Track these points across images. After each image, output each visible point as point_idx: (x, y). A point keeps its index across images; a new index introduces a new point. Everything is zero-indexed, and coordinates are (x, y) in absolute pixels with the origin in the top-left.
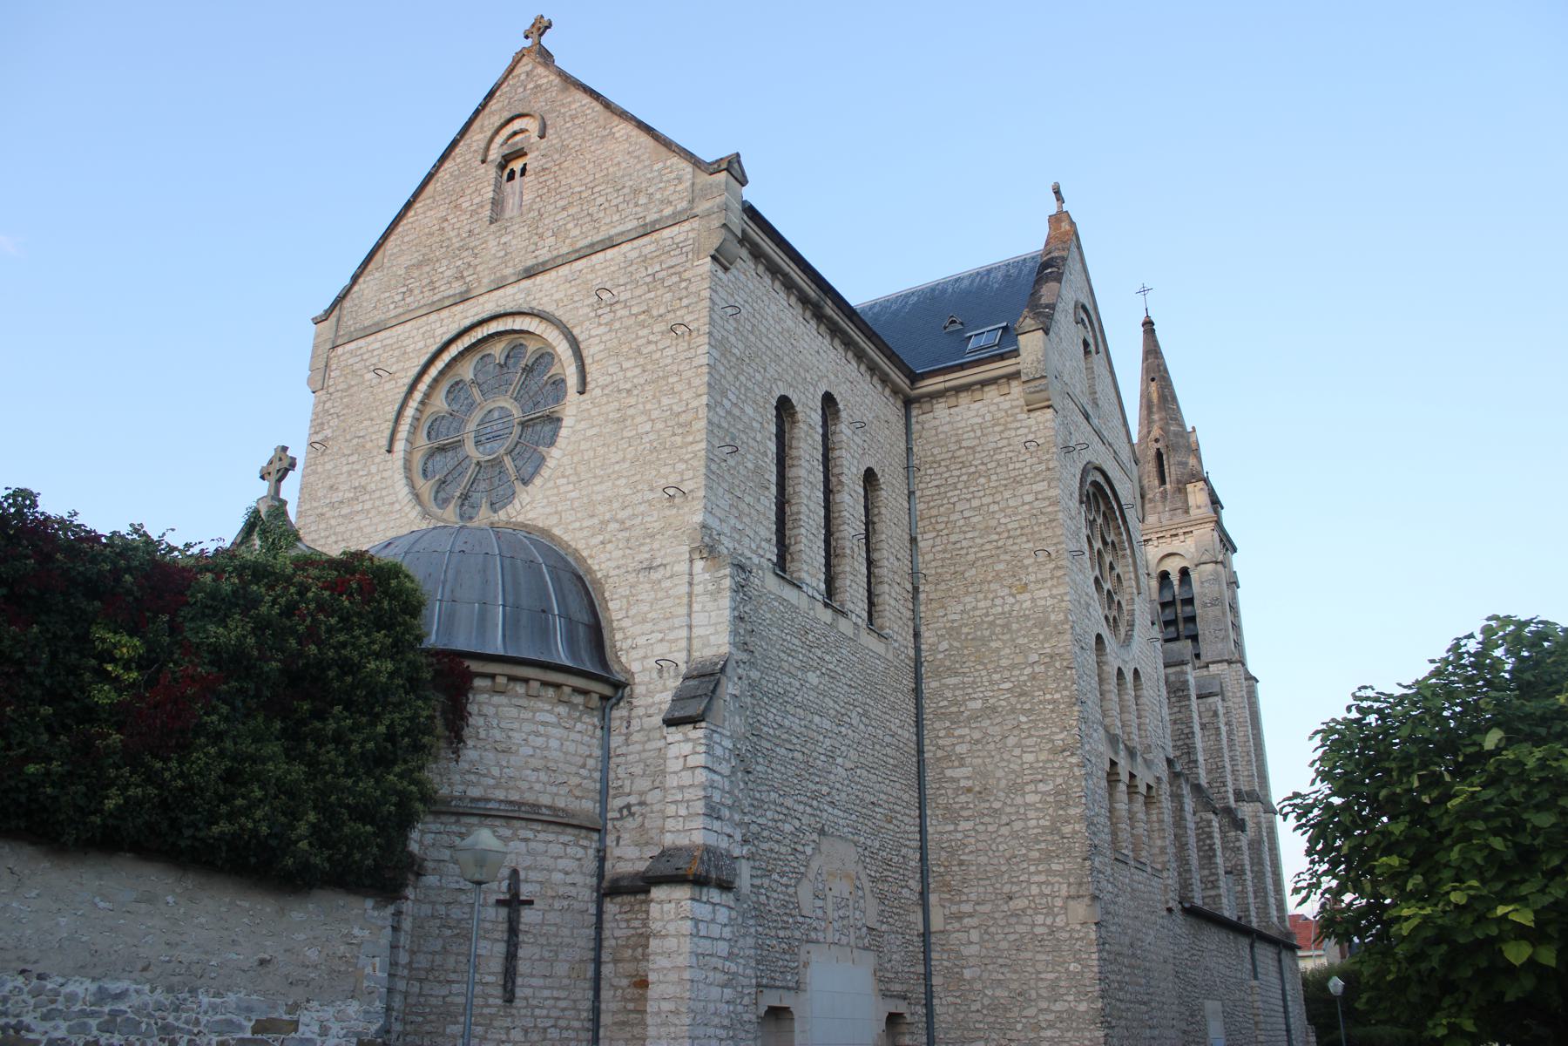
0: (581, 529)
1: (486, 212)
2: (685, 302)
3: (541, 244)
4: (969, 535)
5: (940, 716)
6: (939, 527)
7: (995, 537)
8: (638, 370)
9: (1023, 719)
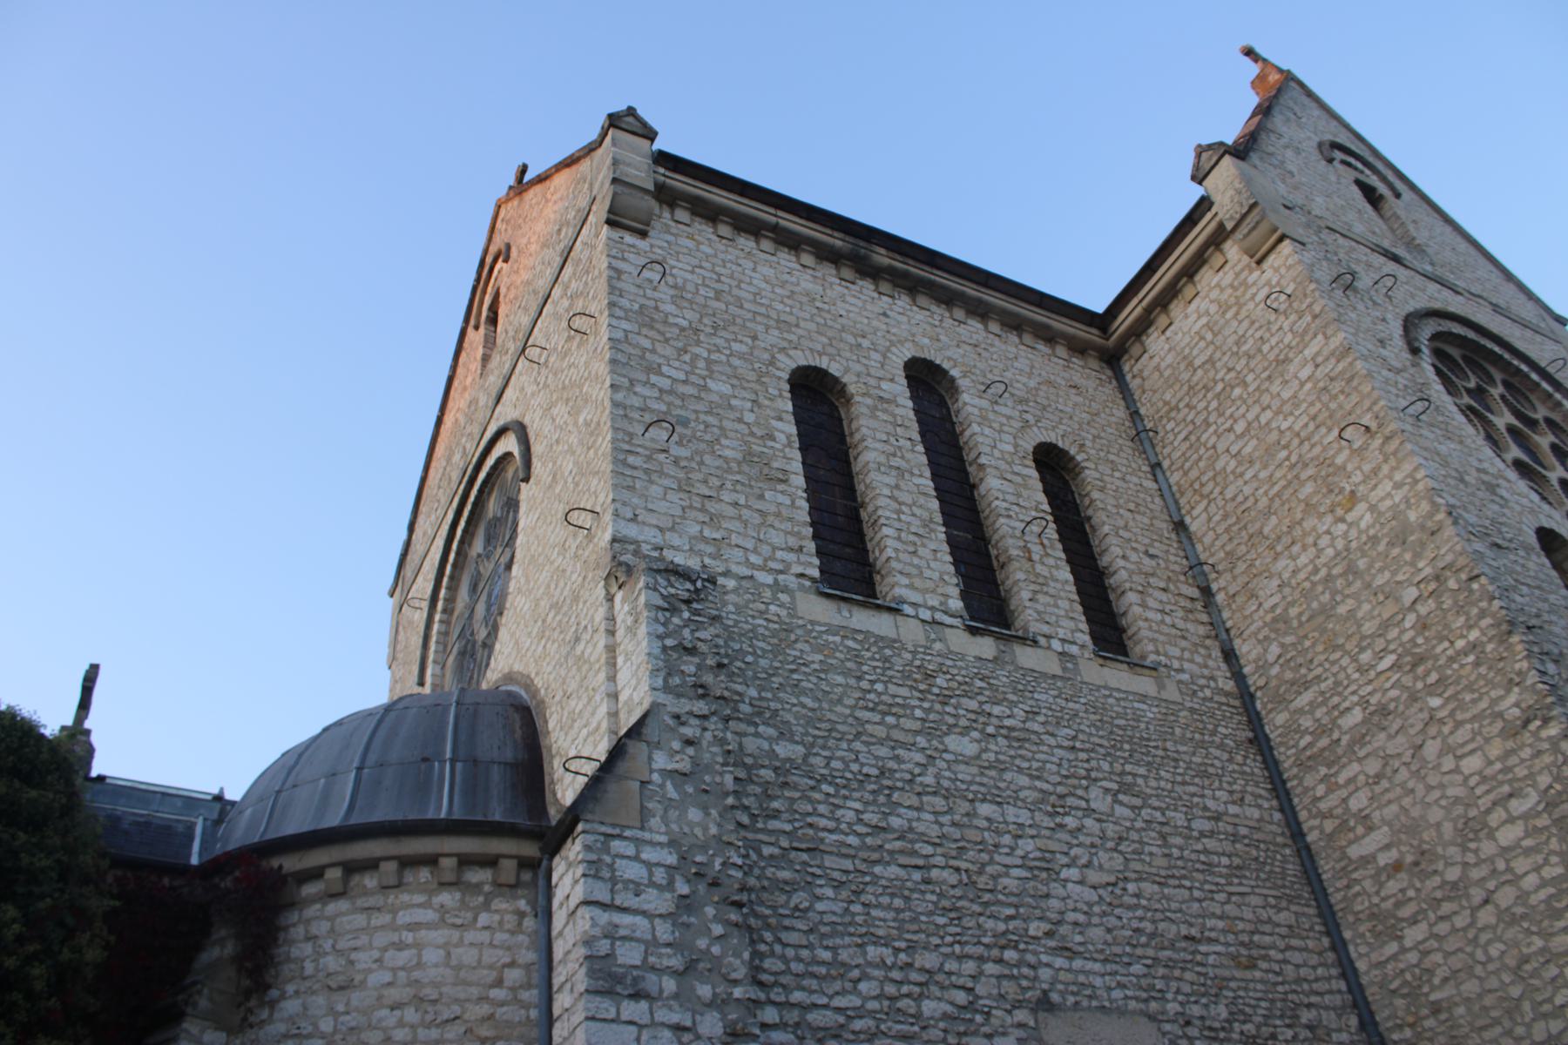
4: (1248, 476)
5: (1306, 764)
6: (1206, 490)
7: (1284, 453)
9: (1435, 702)
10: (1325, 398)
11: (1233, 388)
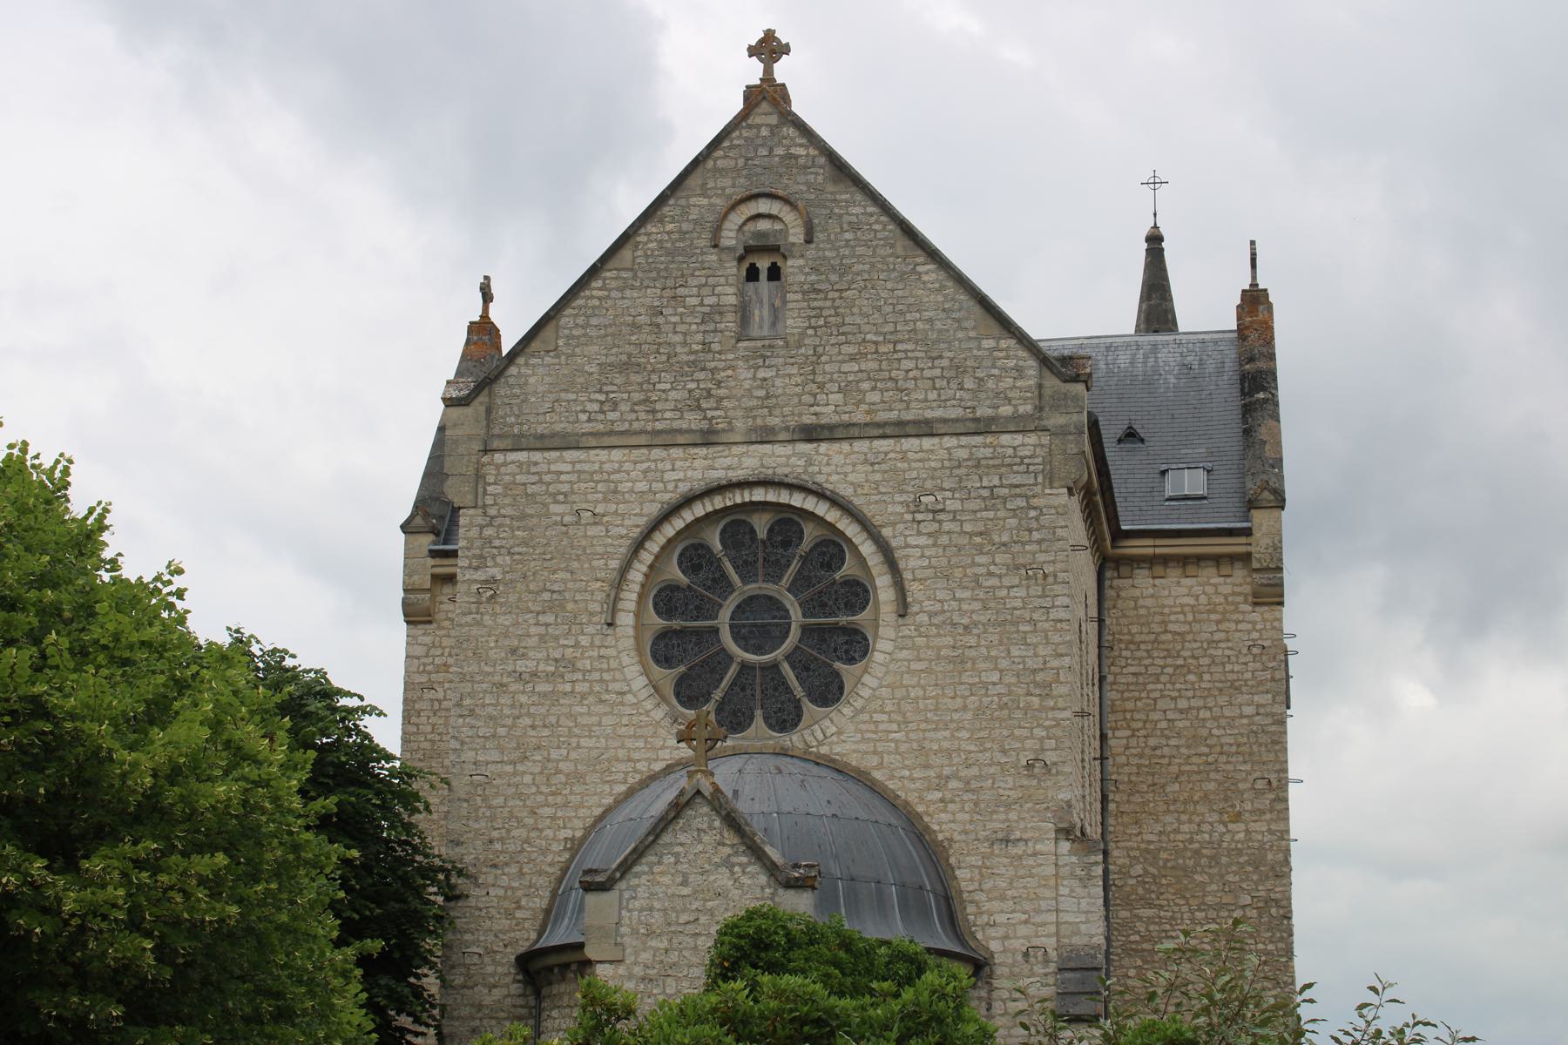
0: (912, 780)
1: (730, 323)
2: (1036, 536)
3: (821, 398)
4: (1173, 742)
5: (1130, 951)
6: (1135, 725)
7: (1206, 750)
8: (977, 605)
10: (1252, 740)
11: (1189, 672)
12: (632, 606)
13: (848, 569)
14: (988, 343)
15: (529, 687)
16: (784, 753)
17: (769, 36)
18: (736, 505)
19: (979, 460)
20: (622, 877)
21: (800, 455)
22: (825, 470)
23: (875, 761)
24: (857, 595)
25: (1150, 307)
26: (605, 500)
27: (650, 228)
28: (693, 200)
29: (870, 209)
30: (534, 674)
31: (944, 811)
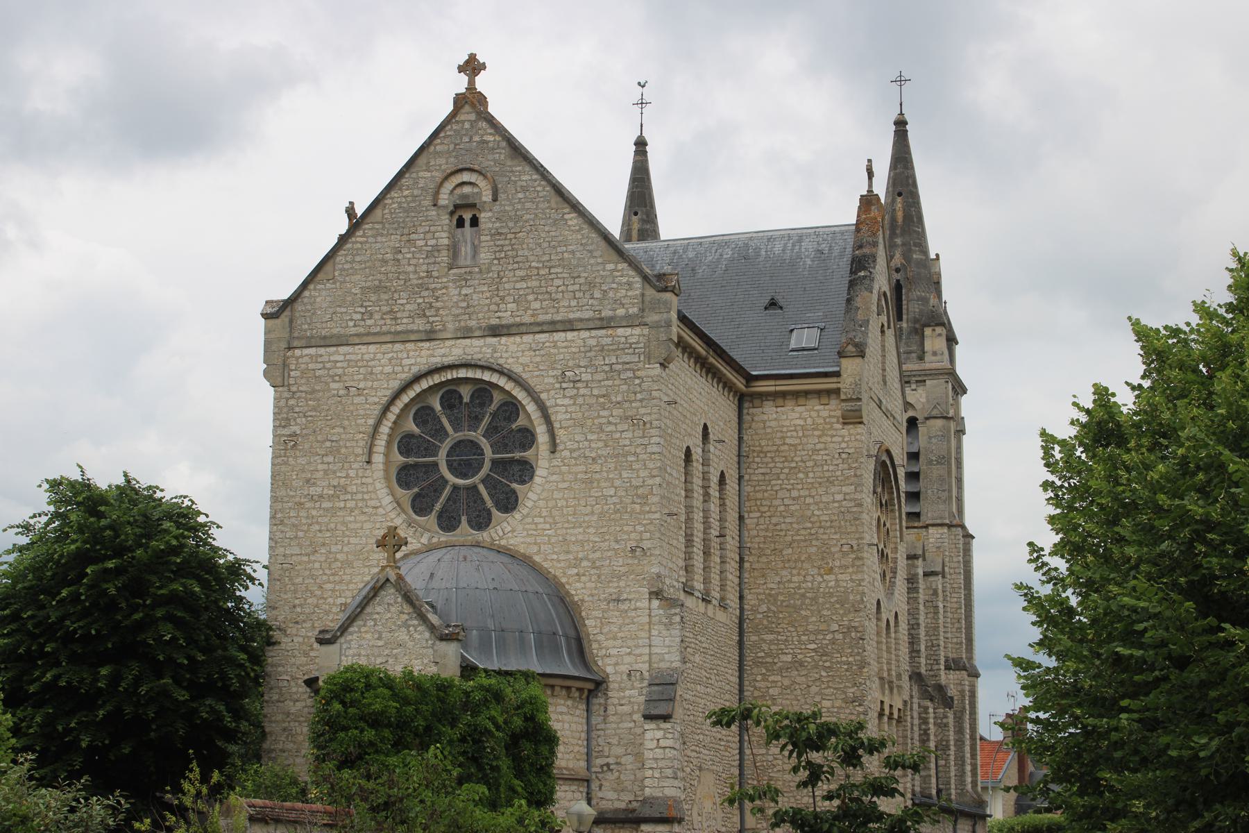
0: (559, 561)
1: (444, 257)
2: (639, 396)
4: (788, 520)
5: (758, 663)
6: (762, 509)
7: (809, 525)
8: (601, 444)
9: (824, 674)
12: (382, 449)
13: (521, 422)
14: (610, 266)
15: (317, 505)
16: (477, 545)
17: (472, 58)
18: (448, 381)
19: (603, 346)
20: (342, 635)
21: (488, 346)
22: (505, 355)
23: (535, 549)
24: (526, 437)
25: (896, 174)
26: (365, 379)
27: (393, 194)
28: (421, 174)
29: (535, 177)
30: (321, 496)
31: (579, 581)
